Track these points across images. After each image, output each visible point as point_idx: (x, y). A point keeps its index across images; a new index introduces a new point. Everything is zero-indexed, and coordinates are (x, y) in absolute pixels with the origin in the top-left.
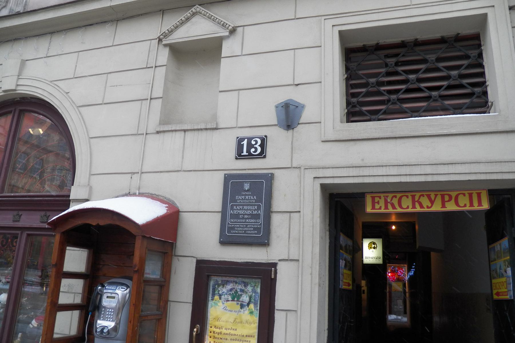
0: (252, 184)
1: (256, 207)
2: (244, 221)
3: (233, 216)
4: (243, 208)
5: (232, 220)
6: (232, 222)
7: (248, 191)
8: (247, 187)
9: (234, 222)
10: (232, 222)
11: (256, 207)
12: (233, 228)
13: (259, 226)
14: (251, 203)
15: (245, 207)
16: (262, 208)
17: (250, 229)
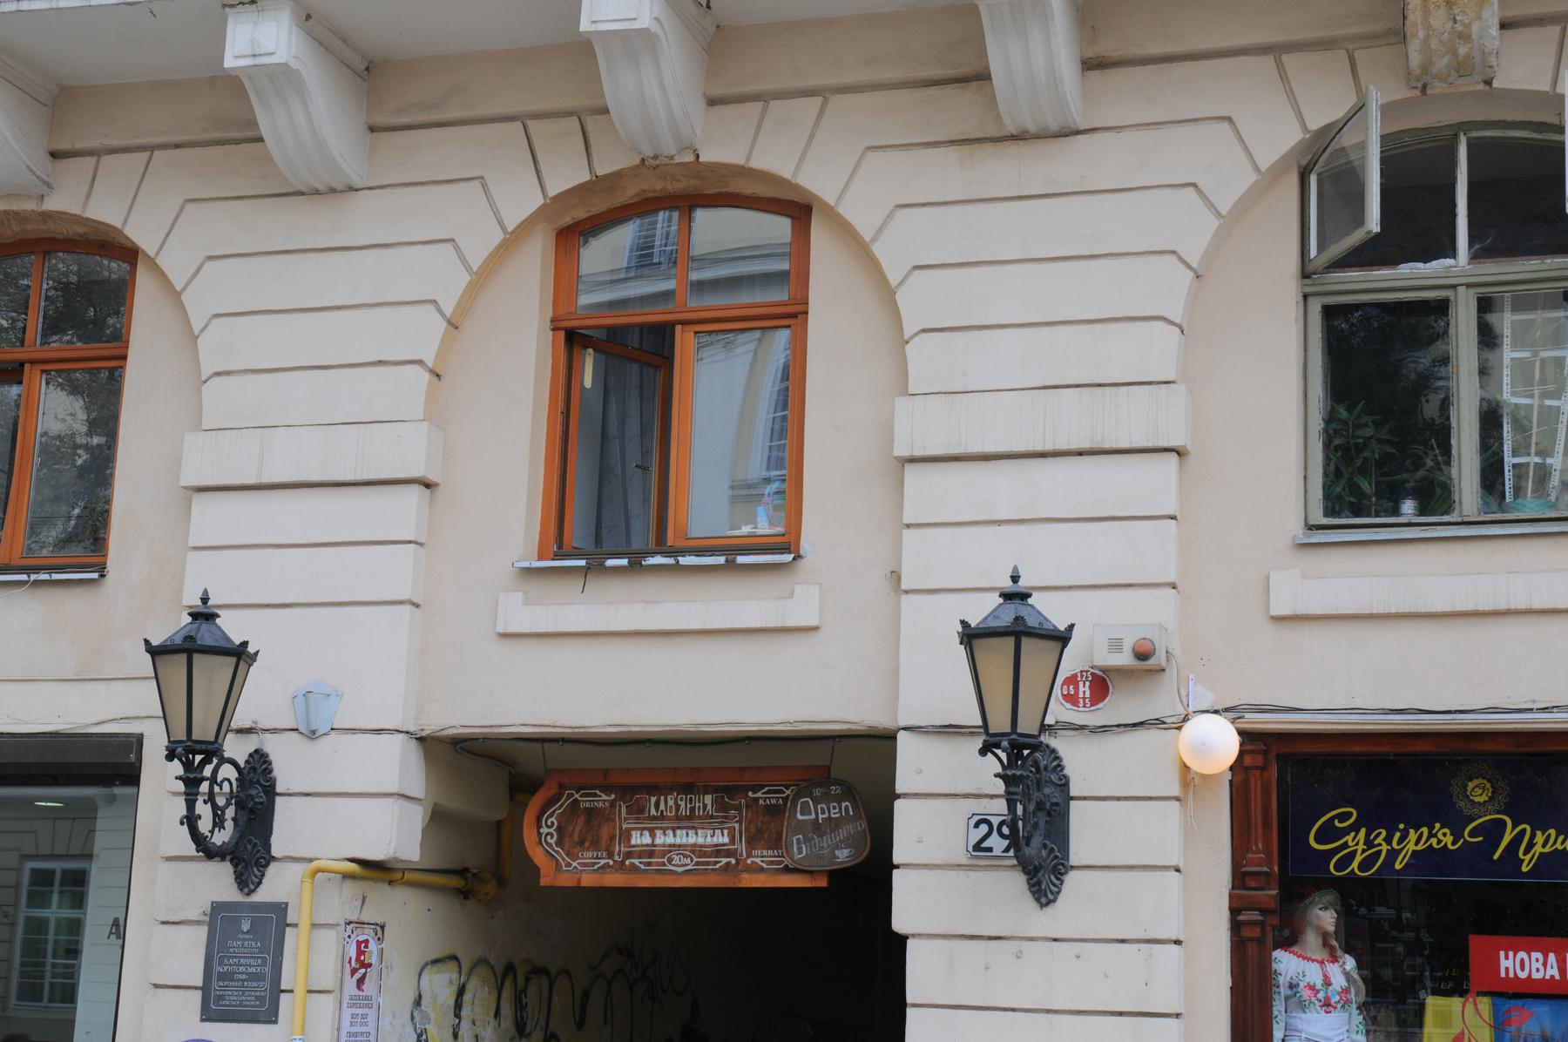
0: (254, 922)
1: (260, 961)
2: (240, 984)
3: (223, 976)
4: (239, 961)
5: (221, 984)
6: (221, 987)
7: (248, 932)
8: (246, 926)
9: (225, 987)
10: (221, 987)
11: (260, 961)
12: (221, 997)
13: (263, 994)
14: (251, 953)
15: (242, 961)
16: (269, 963)
17: (249, 998)
